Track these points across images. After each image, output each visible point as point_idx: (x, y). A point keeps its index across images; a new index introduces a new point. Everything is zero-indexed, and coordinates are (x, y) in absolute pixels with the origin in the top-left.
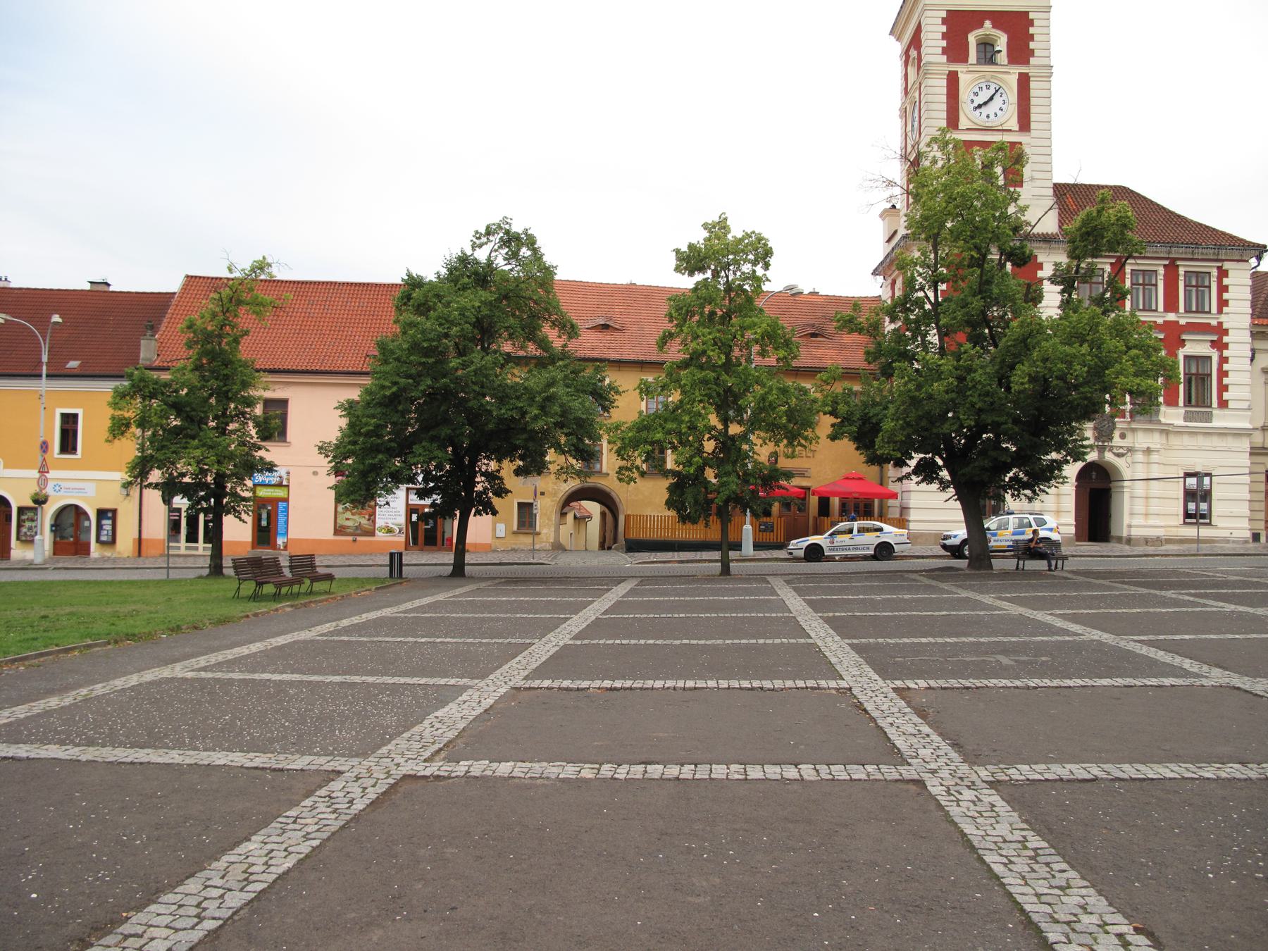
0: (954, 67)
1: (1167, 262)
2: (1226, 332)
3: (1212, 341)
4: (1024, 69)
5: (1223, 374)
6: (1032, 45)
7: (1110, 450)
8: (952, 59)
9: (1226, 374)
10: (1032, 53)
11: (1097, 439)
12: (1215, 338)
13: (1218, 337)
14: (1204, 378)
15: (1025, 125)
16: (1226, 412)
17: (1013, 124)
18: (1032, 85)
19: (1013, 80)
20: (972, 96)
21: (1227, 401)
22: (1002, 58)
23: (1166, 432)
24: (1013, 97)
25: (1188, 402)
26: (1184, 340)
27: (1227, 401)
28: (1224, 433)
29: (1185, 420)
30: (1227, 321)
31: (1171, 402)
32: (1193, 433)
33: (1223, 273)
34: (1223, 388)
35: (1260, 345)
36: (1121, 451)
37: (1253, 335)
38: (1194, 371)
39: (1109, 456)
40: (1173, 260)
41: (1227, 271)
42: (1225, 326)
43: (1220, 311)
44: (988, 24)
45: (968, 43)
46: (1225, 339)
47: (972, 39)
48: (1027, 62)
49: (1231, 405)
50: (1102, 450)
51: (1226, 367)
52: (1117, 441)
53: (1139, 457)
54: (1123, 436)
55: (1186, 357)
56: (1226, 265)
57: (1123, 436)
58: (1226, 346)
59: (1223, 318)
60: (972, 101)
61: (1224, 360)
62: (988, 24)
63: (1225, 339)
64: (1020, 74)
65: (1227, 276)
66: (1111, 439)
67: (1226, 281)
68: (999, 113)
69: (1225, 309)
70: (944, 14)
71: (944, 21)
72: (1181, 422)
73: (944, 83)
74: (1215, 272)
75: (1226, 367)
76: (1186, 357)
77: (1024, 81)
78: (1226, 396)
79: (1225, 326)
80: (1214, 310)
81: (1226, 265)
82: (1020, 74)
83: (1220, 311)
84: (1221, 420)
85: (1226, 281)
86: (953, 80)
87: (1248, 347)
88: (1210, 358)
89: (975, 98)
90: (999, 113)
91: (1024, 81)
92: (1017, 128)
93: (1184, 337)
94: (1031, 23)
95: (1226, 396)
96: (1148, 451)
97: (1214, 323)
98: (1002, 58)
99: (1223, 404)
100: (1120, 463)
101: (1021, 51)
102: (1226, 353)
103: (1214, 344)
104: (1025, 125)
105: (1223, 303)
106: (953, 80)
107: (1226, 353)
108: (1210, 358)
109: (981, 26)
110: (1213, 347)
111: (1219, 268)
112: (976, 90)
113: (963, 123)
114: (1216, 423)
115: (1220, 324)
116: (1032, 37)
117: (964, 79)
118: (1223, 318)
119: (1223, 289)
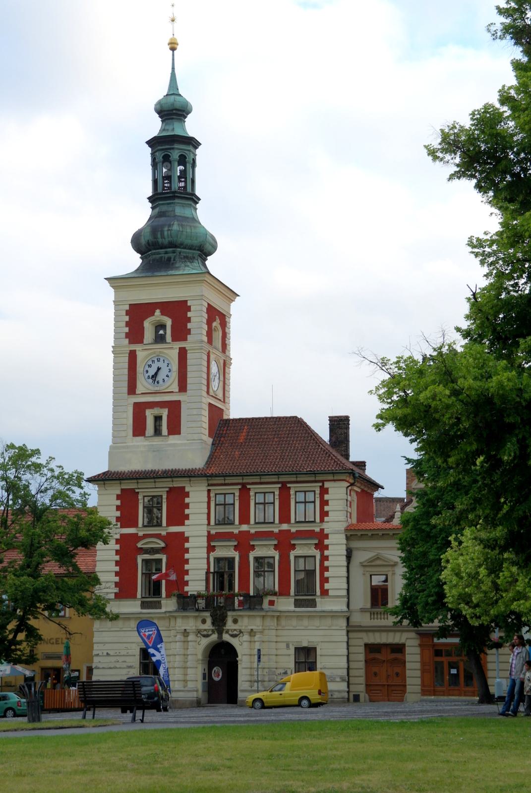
0: (133, 347)
1: (279, 486)
2: (327, 536)
3: (316, 544)
4: (182, 344)
5: (324, 569)
6: (189, 326)
7: (227, 632)
8: (130, 343)
9: (327, 569)
10: (189, 332)
11: (213, 624)
12: (316, 542)
13: (321, 540)
14: (310, 573)
15: (183, 387)
16: (326, 599)
17: (175, 387)
18: (189, 356)
19: (174, 354)
20: (147, 368)
21: (327, 591)
22: (169, 338)
23: (279, 616)
24: (175, 367)
25: (297, 593)
26: (294, 545)
27: (327, 591)
28: (324, 615)
29: (296, 606)
30: (328, 527)
31: (284, 591)
32: (300, 617)
33: (324, 491)
34: (324, 580)
35: (354, 544)
36: (235, 632)
37: (348, 538)
38: (302, 567)
39: (226, 637)
40: (284, 484)
41: (327, 489)
42: (326, 532)
43: (322, 520)
44: (158, 312)
45: (143, 328)
46: (326, 542)
47: (148, 326)
48: (185, 339)
49: (331, 593)
50: (220, 633)
51: (326, 563)
52: (230, 625)
53: (246, 637)
54: (235, 621)
55: (296, 557)
56: (327, 485)
57: (235, 621)
58: (327, 547)
59: (324, 526)
60: (147, 372)
61: (324, 558)
62: (158, 312)
63: (326, 542)
64: (180, 349)
65: (327, 493)
66: (225, 624)
67: (326, 497)
68: (166, 379)
69: (326, 519)
70: (127, 307)
71: (127, 313)
72: (292, 608)
73: (127, 359)
74: (318, 492)
75: (326, 563)
76: (296, 557)
77: (183, 353)
78: (327, 586)
79: (326, 532)
80: (318, 520)
81: (327, 485)
82: (180, 349)
83: (322, 520)
84: (324, 605)
85: (326, 497)
86: (133, 356)
87: (344, 547)
88: (315, 557)
89: (149, 369)
90: (166, 379)
91: (183, 353)
92: (177, 390)
93: (293, 542)
94: (189, 309)
95: (327, 586)
96: (252, 633)
97: (317, 530)
98: (169, 338)
99: (325, 593)
100: (234, 642)
101: (181, 332)
102: (326, 553)
103: (317, 546)
104: (183, 387)
105: (324, 514)
106: (133, 356)
107: (326, 553)
108: (315, 557)
109: (153, 314)
110: (316, 548)
111: (322, 487)
112: (150, 363)
113: (140, 389)
114: (319, 608)
115: (322, 530)
116: (189, 320)
117: (141, 355)
118: (324, 526)
119: (324, 503)
